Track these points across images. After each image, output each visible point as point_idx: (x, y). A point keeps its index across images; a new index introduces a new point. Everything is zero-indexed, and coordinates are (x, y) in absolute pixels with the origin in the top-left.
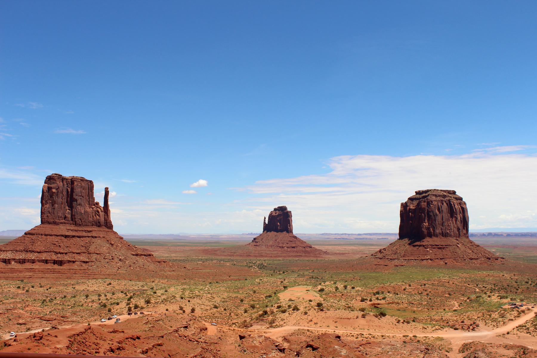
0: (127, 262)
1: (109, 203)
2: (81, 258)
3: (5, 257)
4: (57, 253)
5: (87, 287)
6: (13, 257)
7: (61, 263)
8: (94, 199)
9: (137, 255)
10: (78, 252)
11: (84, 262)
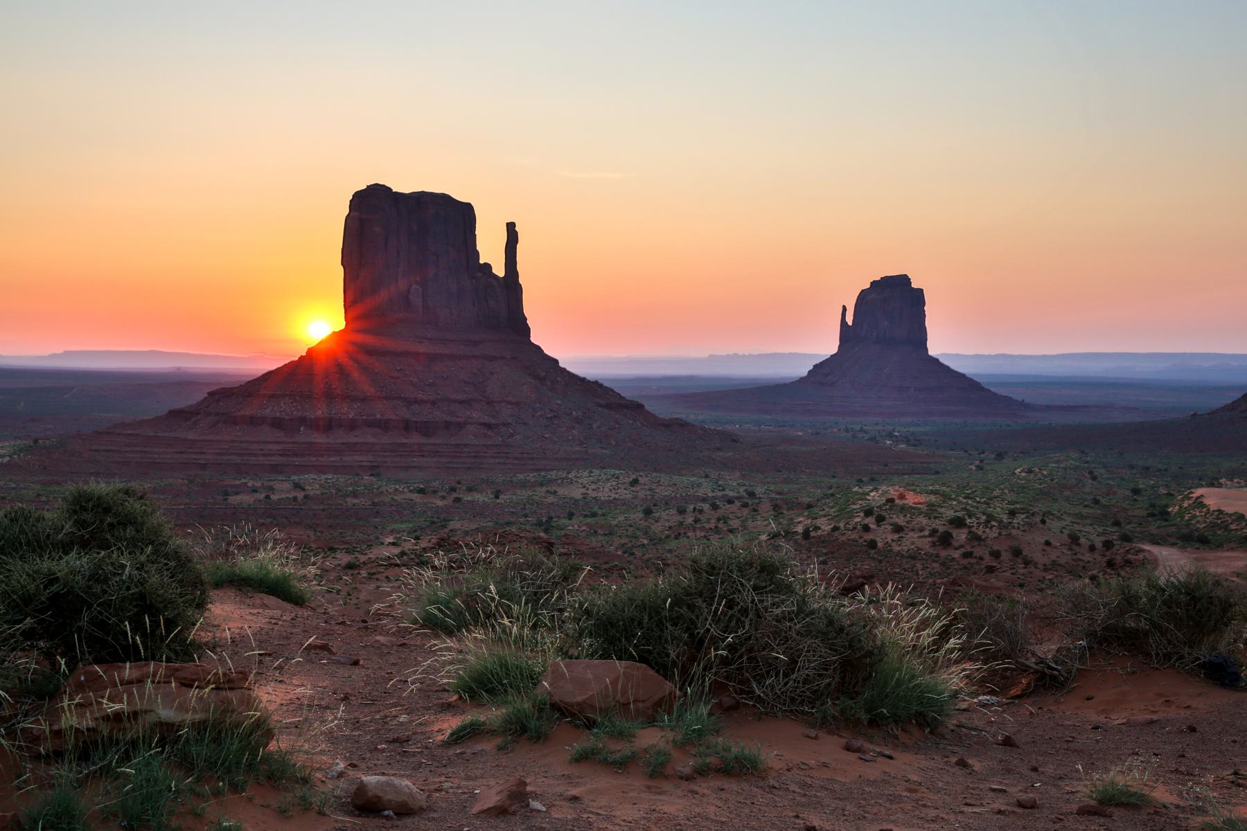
0: (595, 426)
1: (520, 268)
2: (474, 415)
3: (278, 414)
4: (410, 402)
5: (584, 491)
6: (300, 414)
7: (426, 429)
8: (477, 254)
9: (609, 406)
10: (460, 397)
11: (485, 424)
